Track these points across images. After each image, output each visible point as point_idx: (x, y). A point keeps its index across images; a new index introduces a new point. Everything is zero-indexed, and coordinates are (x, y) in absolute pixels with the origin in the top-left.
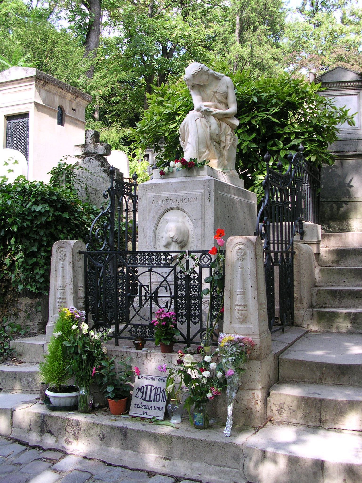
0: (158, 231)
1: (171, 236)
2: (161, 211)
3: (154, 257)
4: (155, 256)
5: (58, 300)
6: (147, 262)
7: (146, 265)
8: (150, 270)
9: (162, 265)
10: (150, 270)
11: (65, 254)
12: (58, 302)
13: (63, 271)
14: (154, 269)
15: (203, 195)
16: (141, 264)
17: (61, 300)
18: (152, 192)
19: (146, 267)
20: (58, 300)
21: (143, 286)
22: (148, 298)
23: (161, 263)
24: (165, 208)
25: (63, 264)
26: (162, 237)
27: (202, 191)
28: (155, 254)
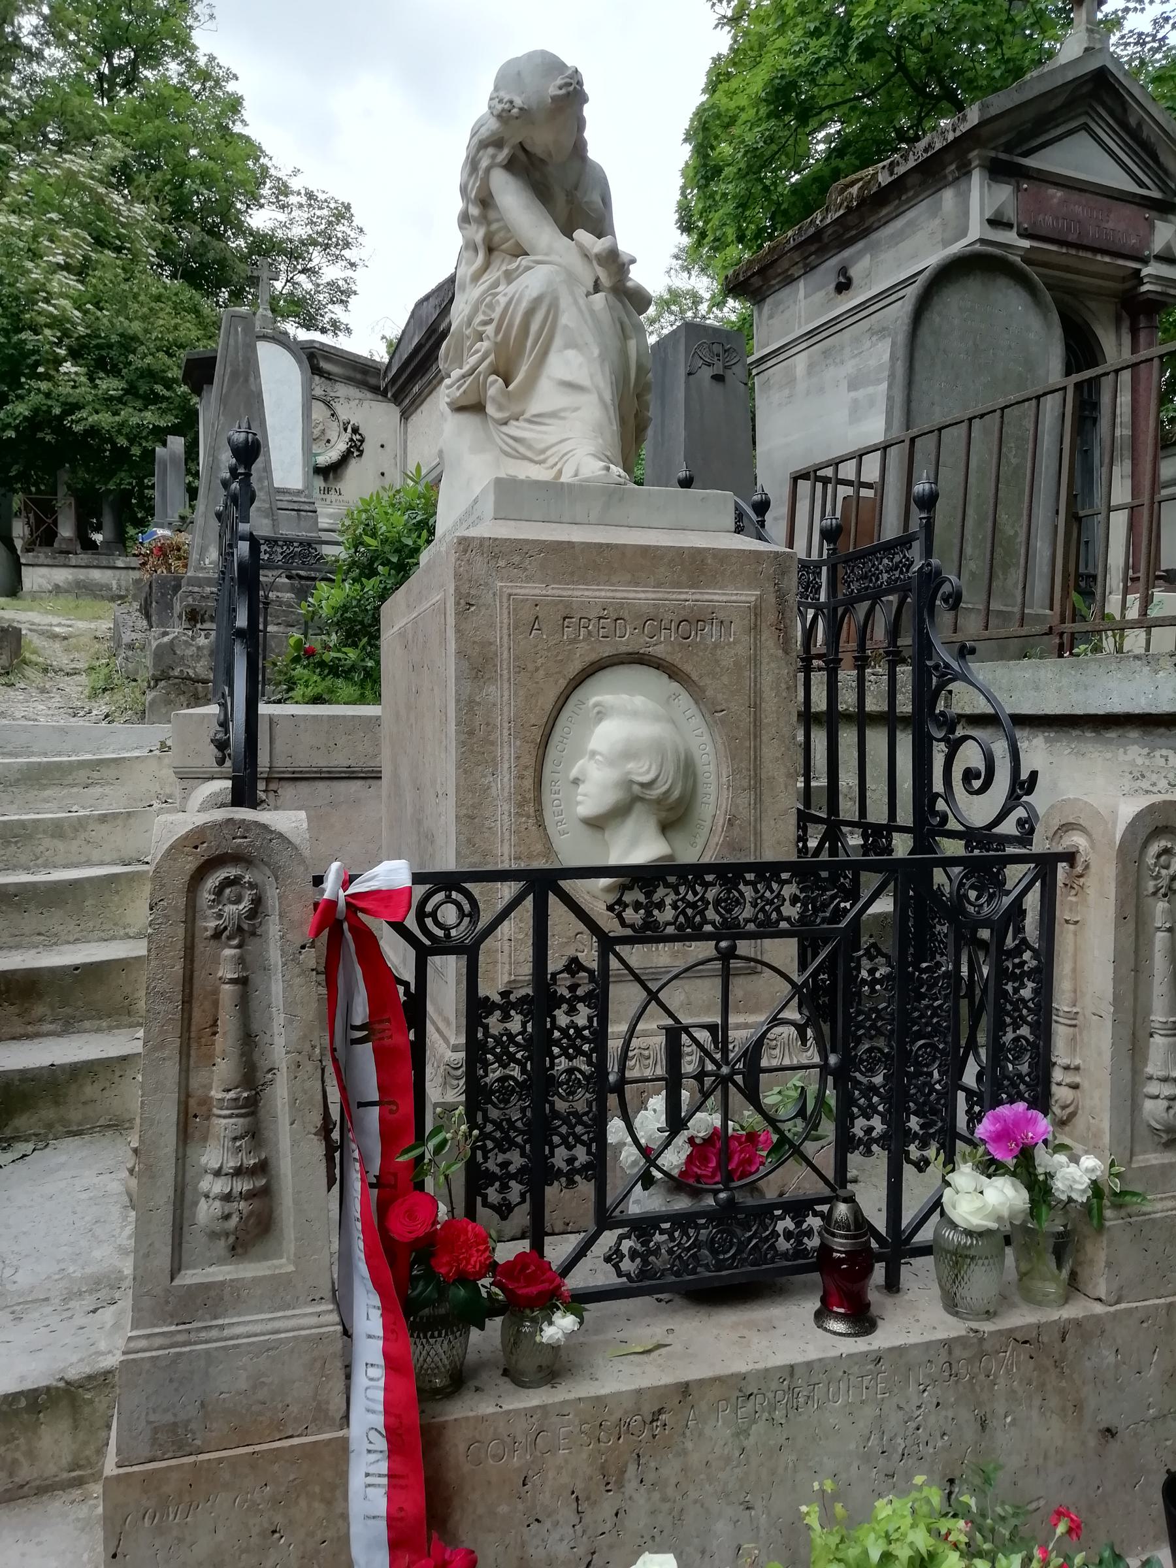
0: (552, 753)
1: (646, 779)
2: (574, 667)
3: (748, 892)
4: (753, 884)
5: (219, 1186)
6: (711, 914)
7: (708, 928)
8: (727, 956)
9: (783, 925)
10: (727, 956)
11: (257, 901)
12: (227, 1198)
13: (244, 1003)
14: (744, 947)
15: (756, 610)
16: (680, 928)
17: (243, 1185)
18: (529, 579)
19: (707, 937)
20: (219, 1186)
21: (686, 1029)
22: (708, 1081)
23: (781, 918)
24: (594, 657)
25: (241, 961)
26: (576, 782)
27: (749, 596)
28: (750, 876)
